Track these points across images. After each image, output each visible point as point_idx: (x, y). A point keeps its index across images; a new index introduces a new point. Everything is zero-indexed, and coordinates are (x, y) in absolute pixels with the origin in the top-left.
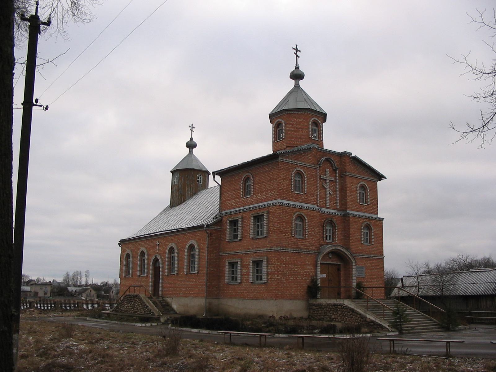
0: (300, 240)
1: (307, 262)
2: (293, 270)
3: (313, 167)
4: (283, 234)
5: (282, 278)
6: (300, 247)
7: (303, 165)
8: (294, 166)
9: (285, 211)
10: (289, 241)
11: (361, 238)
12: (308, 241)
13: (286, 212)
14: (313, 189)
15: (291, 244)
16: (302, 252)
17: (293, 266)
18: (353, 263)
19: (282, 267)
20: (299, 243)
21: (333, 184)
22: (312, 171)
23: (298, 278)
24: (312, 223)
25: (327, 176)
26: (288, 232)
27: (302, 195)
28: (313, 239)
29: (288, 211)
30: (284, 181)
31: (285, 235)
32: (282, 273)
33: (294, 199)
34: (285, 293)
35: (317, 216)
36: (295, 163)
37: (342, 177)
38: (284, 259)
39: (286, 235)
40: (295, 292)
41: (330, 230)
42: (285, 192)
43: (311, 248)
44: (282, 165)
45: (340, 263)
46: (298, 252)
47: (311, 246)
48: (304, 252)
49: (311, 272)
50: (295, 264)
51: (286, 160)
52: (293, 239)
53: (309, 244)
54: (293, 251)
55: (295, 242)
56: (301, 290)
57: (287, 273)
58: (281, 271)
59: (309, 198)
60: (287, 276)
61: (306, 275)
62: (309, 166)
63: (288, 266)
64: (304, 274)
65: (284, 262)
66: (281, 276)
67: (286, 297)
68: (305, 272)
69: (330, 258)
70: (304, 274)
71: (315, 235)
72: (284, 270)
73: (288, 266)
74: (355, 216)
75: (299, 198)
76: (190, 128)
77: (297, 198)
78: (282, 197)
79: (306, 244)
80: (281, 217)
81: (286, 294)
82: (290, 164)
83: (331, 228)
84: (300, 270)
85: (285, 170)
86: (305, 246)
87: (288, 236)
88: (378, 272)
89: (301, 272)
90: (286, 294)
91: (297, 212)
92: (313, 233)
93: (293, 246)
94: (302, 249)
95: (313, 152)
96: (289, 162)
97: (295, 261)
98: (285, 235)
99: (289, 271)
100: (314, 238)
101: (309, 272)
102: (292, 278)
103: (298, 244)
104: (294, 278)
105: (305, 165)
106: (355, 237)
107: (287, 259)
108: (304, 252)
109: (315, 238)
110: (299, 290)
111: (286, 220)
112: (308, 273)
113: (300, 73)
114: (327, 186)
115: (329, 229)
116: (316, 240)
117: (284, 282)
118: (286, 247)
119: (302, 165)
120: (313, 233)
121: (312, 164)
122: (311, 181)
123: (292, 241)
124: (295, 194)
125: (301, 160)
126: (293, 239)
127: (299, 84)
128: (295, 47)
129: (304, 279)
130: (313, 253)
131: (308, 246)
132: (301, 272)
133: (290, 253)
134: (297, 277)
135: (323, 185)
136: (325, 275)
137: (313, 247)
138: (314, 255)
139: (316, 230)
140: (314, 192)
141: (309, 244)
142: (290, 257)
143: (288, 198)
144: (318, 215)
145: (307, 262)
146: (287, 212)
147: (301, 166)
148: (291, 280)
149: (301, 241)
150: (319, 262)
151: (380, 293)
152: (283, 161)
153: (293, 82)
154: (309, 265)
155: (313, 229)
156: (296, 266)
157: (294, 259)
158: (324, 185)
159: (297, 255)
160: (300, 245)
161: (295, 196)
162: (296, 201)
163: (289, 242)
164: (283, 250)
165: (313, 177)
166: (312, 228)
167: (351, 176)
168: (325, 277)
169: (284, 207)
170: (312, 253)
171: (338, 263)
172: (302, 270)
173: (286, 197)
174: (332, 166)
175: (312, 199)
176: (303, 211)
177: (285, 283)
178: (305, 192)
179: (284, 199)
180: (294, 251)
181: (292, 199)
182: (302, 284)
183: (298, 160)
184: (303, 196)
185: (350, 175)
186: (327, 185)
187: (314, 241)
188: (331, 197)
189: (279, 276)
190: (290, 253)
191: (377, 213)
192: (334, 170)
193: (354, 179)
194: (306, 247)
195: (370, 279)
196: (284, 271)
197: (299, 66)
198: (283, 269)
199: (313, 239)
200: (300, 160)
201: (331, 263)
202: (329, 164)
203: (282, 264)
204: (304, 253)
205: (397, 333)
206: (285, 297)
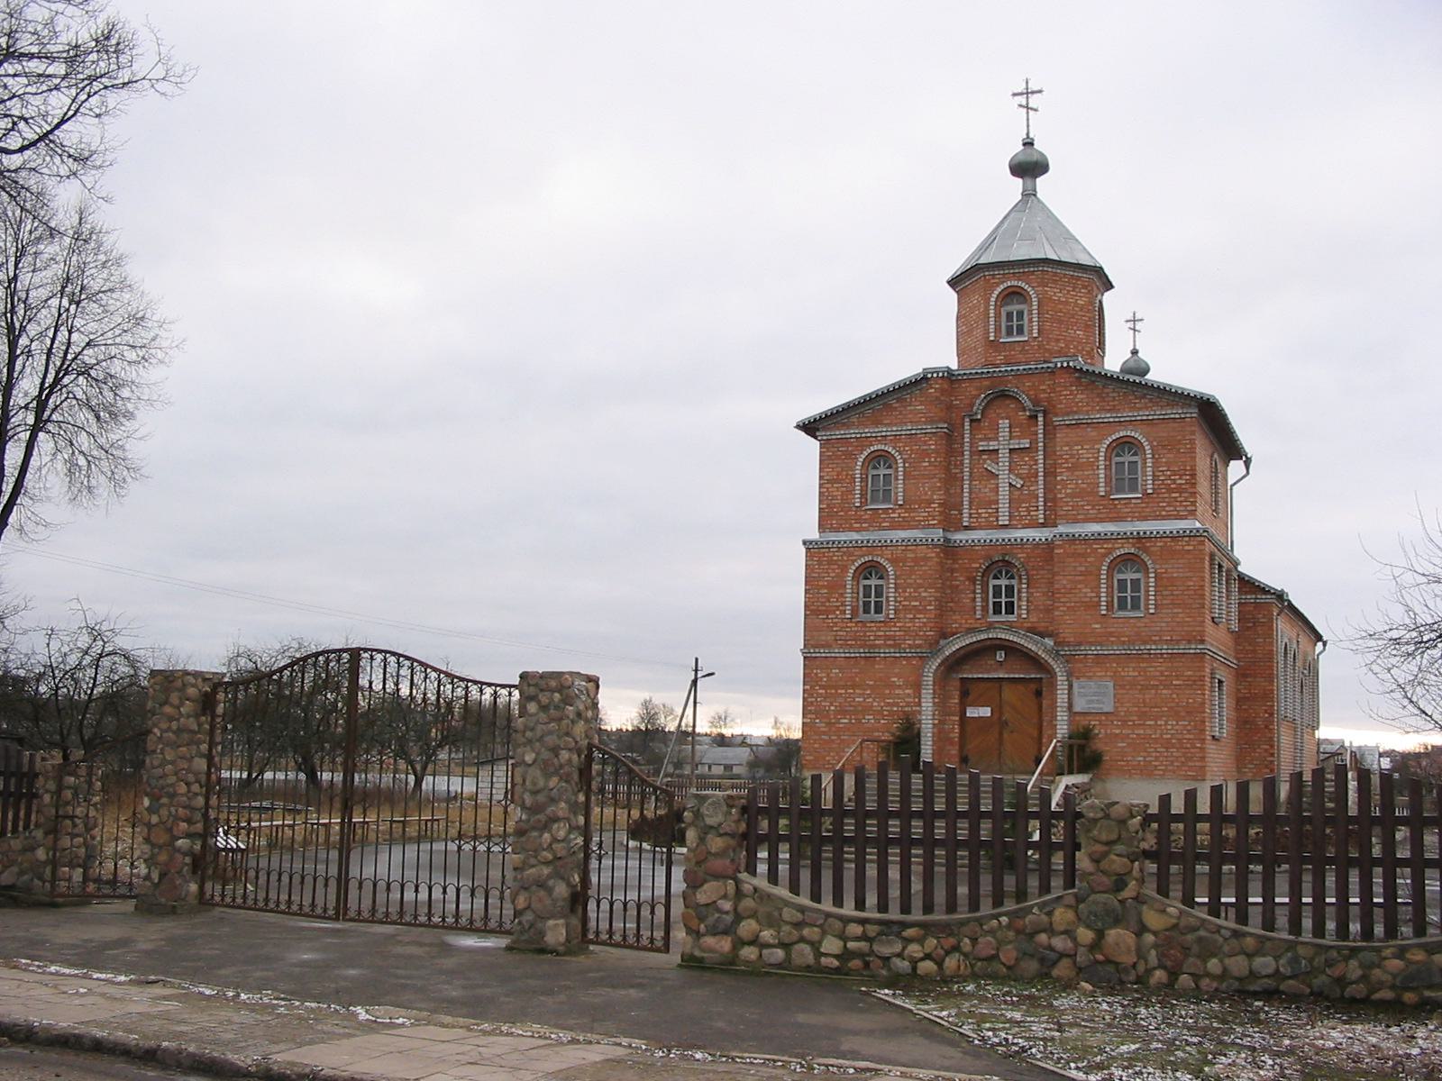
8: (863, 442)
11: (1100, 597)
13: (830, 562)
19: (817, 694)
28: (915, 618)
35: (926, 559)
37: (1050, 430)
45: (1038, 676)
57: (832, 708)
61: (891, 713)
62: (913, 432)
74: (1073, 539)
76: (1131, 325)
77: (875, 520)
84: (870, 700)
85: (838, 457)
86: (888, 638)
88: (1175, 696)
89: (875, 704)
91: (863, 556)
92: (917, 603)
94: (879, 646)
102: (846, 721)
103: (865, 636)
106: (1077, 599)
109: (922, 616)
112: (898, 707)
113: (1035, 157)
114: (1002, 467)
115: (1006, 586)
118: (829, 646)
120: (917, 603)
121: (925, 423)
128: (1032, 87)
136: (989, 709)
137: (914, 640)
139: (923, 594)
140: (932, 495)
141: (902, 633)
151: (1183, 759)
159: (863, 663)
161: (867, 517)
171: (1033, 676)
177: (824, 733)
178: (897, 500)
181: (858, 525)
183: (877, 423)
184: (894, 513)
195: (1135, 718)
197: (1033, 139)
201: (1006, 676)
202: (1012, 406)
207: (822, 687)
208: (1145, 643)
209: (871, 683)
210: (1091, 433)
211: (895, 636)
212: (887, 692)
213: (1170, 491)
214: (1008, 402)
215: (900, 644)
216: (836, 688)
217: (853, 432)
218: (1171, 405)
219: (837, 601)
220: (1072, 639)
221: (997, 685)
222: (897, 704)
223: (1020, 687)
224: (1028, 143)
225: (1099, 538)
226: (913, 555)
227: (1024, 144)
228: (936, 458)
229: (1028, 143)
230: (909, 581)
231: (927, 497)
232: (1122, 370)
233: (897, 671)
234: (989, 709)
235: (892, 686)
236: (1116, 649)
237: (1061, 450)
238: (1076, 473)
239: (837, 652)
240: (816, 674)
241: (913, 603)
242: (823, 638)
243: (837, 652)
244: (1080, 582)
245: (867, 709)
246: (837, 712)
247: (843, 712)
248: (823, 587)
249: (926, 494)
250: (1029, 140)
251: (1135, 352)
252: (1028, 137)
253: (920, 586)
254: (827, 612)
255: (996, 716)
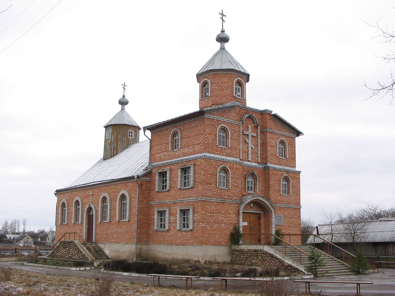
0: (224, 190)
1: (230, 211)
2: (217, 218)
3: (237, 124)
4: (208, 185)
5: (207, 226)
6: (223, 197)
7: (227, 122)
8: (219, 122)
9: (210, 163)
10: (213, 191)
11: (280, 189)
12: (231, 191)
13: (211, 165)
14: (236, 144)
15: (215, 194)
16: (226, 202)
17: (218, 215)
18: (273, 212)
19: (207, 215)
20: (223, 194)
21: (254, 140)
22: (235, 127)
23: (221, 226)
24: (235, 175)
25: (249, 131)
26: (213, 183)
27: (226, 149)
28: (236, 189)
29: (213, 164)
30: (210, 136)
31: (210, 185)
32: (207, 221)
33: (218, 153)
34: (210, 240)
35: (239, 169)
36: (220, 120)
37: (263, 133)
38: (209, 208)
39: (211, 186)
40: (219, 239)
41: (252, 182)
42: (210, 146)
43: (234, 198)
44: (208, 121)
46: (222, 201)
47: (234, 196)
48: (227, 202)
49: (234, 220)
50: (219, 213)
51: (212, 117)
52: (217, 190)
53: (232, 195)
54: (217, 201)
55: (219, 192)
56: (224, 237)
57: (212, 221)
58: (206, 220)
59: (232, 152)
60: (212, 224)
61: (230, 224)
62: (233, 123)
63: (212, 214)
64: (227, 222)
65: (209, 211)
66: (206, 224)
67: (210, 243)
68: (229, 220)
69: (252, 207)
70: (227, 222)
71: (237, 186)
72: (208, 218)
73: (212, 214)
74: (274, 169)
75: (223, 152)
76: (123, 86)
77: (221, 152)
78: (208, 151)
79: (229, 194)
80: (207, 169)
81: (210, 240)
82: (215, 120)
83: (253, 180)
84: (224, 218)
85: (211, 125)
87: (213, 186)
89: (225, 220)
90: (210, 240)
91: (221, 165)
92: (236, 184)
93: (217, 196)
95: (237, 110)
96: (214, 118)
97: (220, 210)
98: (210, 186)
99: (214, 219)
100: (237, 189)
101: (232, 220)
102: (216, 226)
103: (222, 194)
104: (218, 226)
105: (229, 122)
106: (275, 189)
107: (212, 208)
108: (227, 202)
109: (238, 189)
110: (222, 237)
111: (210, 172)
112: (231, 221)
113: (225, 36)
114: (249, 141)
116: (238, 191)
117: (209, 229)
119: (226, 121)
121: (235, 120)
122: (235, 136)
123: (217, 191)
124: (220, 148)
125: (225, 117)
126: (217, 190)
127: (224, 47)
128: (221, 12)
129: (227, 226)
130: (236, 203)
131: (231, 196)
132: (225, 220)
133: (214, 202)
134: (221, 225)
135: (245, 140)
136: (247, 223)
137: (236, 197)
138: (236, 204)
139: (238, 181)
141: (232, 195)
142: (214, 206)
143: (213, 152)
144: (241, 168)
145: (230, 211)
146: (212, 164)
147: (225, 123)
148: (215, 228)
149: (225, 192)
150: (241, 211)
151: (297, 240)
152: (209, 117)
153: (218, 45)
154: (231, 214)
155: (236, 181)
156: (220, 215)
157: (218, 209)
158: (246, 140)
159: (221, 204)
160: (224, 195)
162: (220, 155)
163: (214, 192)
164: (208, 200)
165: (237, 133)
166: (235, 179)
167: (271, 132)
168: (247, 225)
169: (209, 160)
170: (235, 203)
171: (259, 212)
172: (225, 218)
173: (212, 151)
174: (254, 123)
175: (236, 153)
176: (227, 164)
178: (228, 146)
179: (210, 153)
180: (218, 201)
181: (217, 152)
182: (225, 231)
183: (222, 116)
184: (227, 150)
185: (270, 131)
186: (249, 140)
187: (236, 192)
188: (253, 151)
189: (205, 224)
190: (215, 202)
191: (295, 167)
192: (255, 126)
193: (274, 135)
194: (229, 198)
195: (287, 227)
196: (209, 219)
197: (224, 30)
198: (208, 217)
199: (236, 189)
200: (224, 116)
202: (251, 121)
203: (207, 213)
204: (228, 203)
205: (313, 276)
206: (209, 243)
207: (209, 213)
208: (289, 204)
209: (224, 212)
210: (275, 136)
211: (230, 195)
212: (228, 215)
213: (291, 159)
214: (250, 119)
215: (232, 198)
216: (213, 213)
217: (216, 117)
218: (291, 133)
219: (213, 180)
220: (274, 201)
221: (249, 215)
222: (231, 220)
223: (255, 216)
224: (223, 31)
225: (280, 170)
226: (235, 167)
227: (222, 32)
228: (238, 134)
229: (223, 31)
230: (234, 176)
231: (236, 147)
232: (200, 109)
233: (231, 208)
234: (247, 223)
235: (230, 214)
236: (284, 206)
237: (268, 140)
238: (272, 148)
239: (214, 200)
240: (207, 207)
241: (235, 184)
242: (209, 194)
243: (214, 200)
244: (276, 183)
245: (222, 222)
246: (214, 223)
247: (216, 223)
248: (209, 174)
249: (235, 145)
250: (223, 30)
251: (124, 96)
252: (223, 29)
253: (237, 178)
254: (211, 184)
255: (249, 225)
